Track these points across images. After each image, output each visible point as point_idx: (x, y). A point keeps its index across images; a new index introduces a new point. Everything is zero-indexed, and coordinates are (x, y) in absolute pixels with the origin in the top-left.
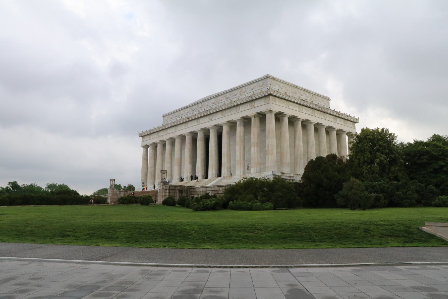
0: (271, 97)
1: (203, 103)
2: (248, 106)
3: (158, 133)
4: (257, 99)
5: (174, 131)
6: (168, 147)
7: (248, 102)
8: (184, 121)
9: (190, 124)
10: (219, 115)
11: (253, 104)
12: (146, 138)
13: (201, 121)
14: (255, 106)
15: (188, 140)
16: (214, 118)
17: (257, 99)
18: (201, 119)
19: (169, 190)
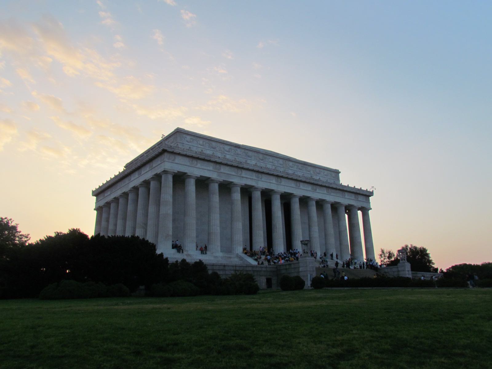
1: (265, 156)
2: (353, 196)
3: (218, 166)
5: (254, 178)
9: (284, 182)
10: (325, 191)
13: (302, 186)
16: (318, 191)
18: (302, 184)
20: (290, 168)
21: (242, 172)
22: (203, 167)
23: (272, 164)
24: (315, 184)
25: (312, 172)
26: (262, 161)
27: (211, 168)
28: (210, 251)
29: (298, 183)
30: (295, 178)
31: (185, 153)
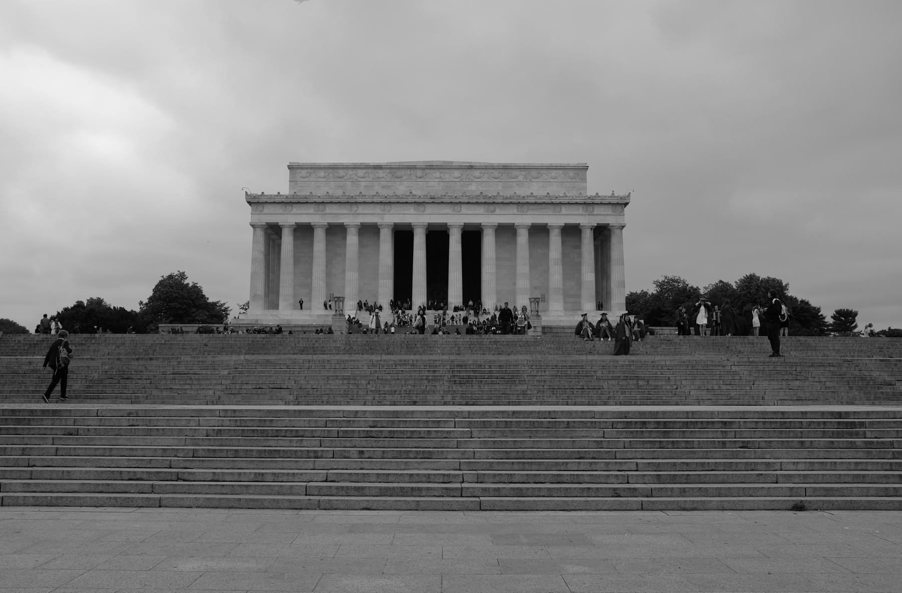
1: (427, 171)
2: (581, 210)
3: (321, 207)
6: (352, 239)
8: (417, 200)
9: (429, 209)
10: (514, 210)
11: (590, 208)
12: (268, 209)
13: (464, 209)
14: (595, 213)
16: (498, 211)
18: (463, 206)
24: (490, 203)
25: (521, 178)
27: (312, 211)
28: (310, 308)
29: (457, 207)
30: (448, 201)
31: (272, 200)
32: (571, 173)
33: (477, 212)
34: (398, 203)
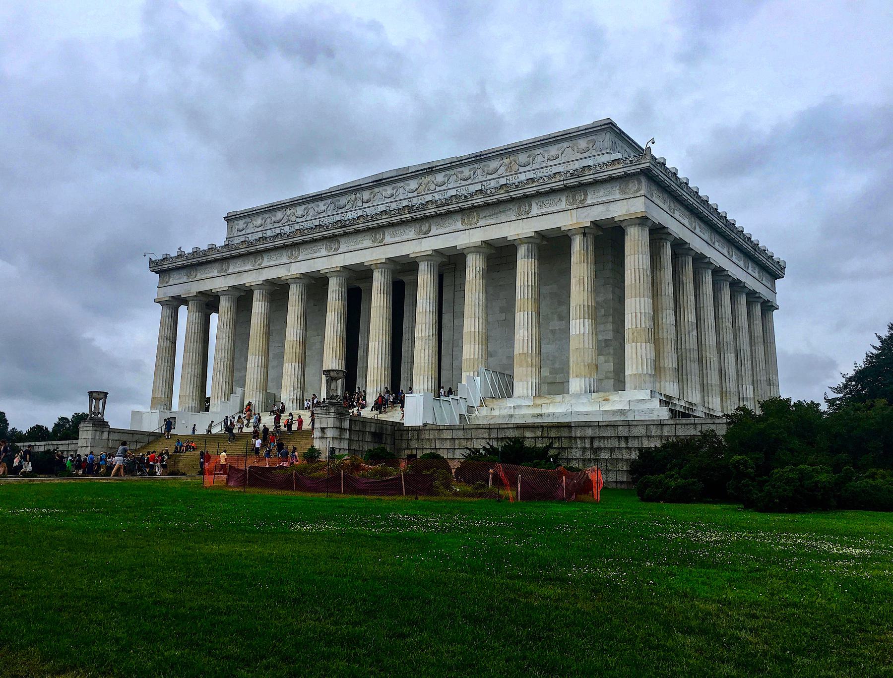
0: (643, 180)
1: (376, 190)
3: (225, 266)
4: (596, 183)
6: (259, 307)
7: (566, 189)
12: (175, 278)
15: (335, 292)
17: (596, 183)
19: (350, 430)
20: (438, 189)
21: (263, 258)
22: (203, 276)
23: (389, 200)
26: (367, 205)
32: (582, 143)
33: (405, 237)
34: (304, 243)
